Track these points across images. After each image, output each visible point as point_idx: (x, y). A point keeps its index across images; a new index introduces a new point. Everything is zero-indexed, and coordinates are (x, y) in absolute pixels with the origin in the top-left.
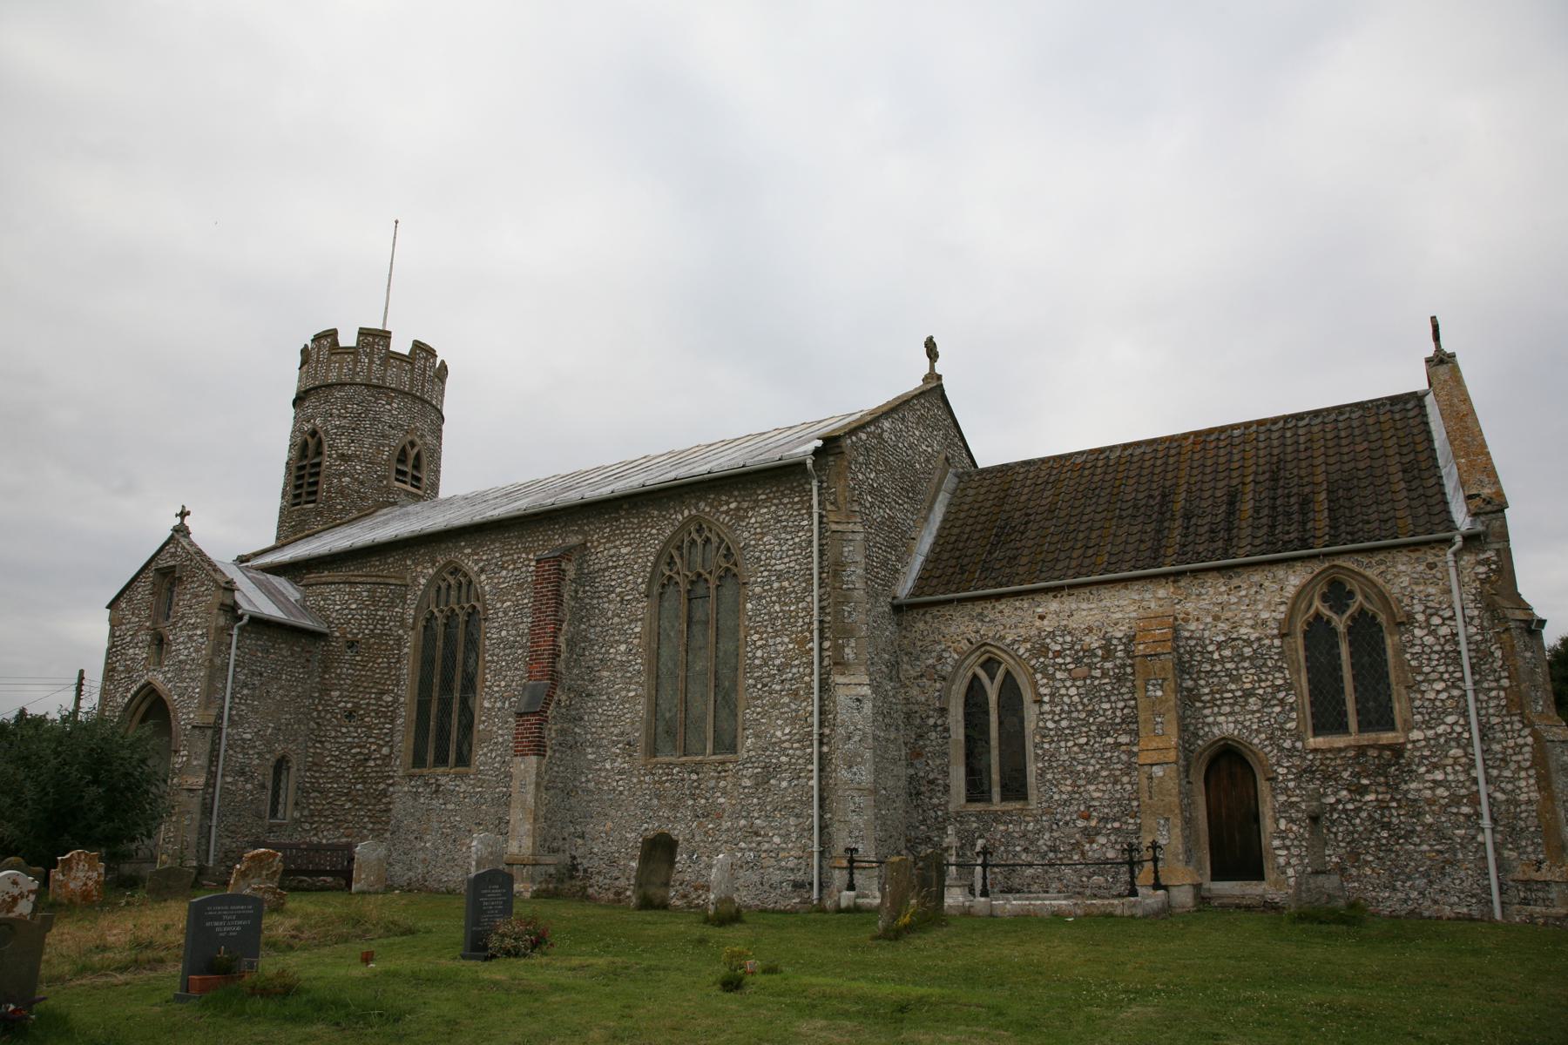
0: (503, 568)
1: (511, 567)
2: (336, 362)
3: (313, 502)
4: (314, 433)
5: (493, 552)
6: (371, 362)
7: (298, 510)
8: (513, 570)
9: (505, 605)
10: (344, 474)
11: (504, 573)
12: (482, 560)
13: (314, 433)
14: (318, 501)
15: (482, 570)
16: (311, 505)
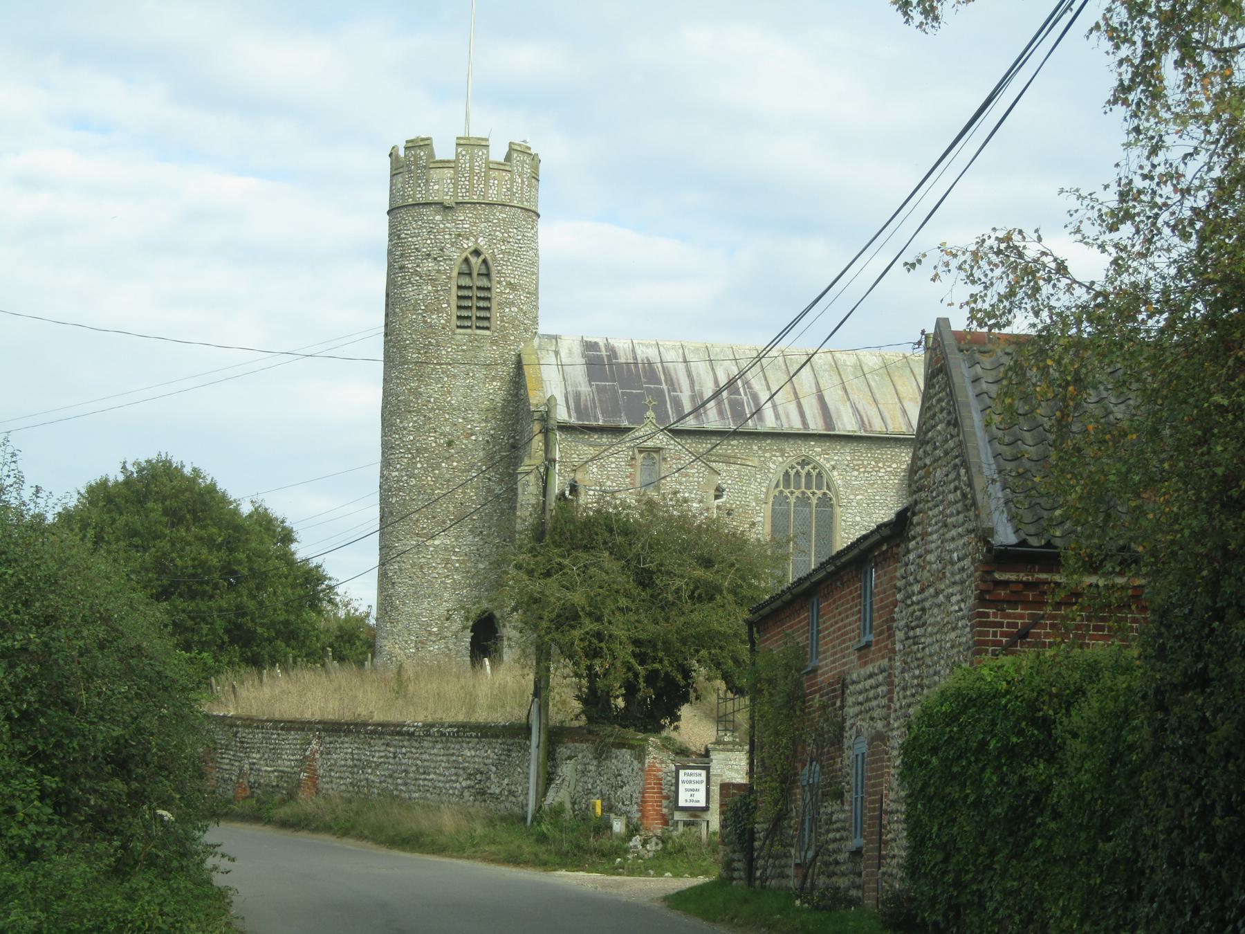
0: (854, 469)
1: (862, 470)
2: (495, 179)
3: (487, 328)
4: (477, 253)
5: (843, 455)
6: (523, 182)
7: (470, 335)
8: (864, 472)
9: (858, 497)
10: (512, 304)
11: (856, 473)
12: (833, 459)
13: (477, 253)
14: (493, 329)
15: (834, 468)
16: (487, 333)
